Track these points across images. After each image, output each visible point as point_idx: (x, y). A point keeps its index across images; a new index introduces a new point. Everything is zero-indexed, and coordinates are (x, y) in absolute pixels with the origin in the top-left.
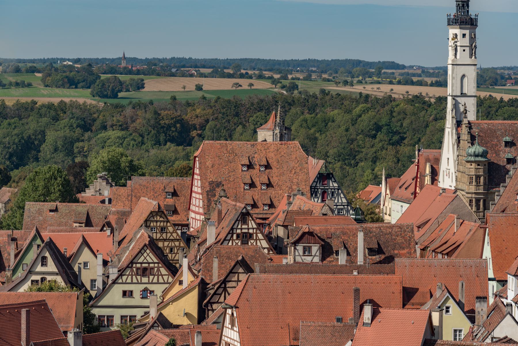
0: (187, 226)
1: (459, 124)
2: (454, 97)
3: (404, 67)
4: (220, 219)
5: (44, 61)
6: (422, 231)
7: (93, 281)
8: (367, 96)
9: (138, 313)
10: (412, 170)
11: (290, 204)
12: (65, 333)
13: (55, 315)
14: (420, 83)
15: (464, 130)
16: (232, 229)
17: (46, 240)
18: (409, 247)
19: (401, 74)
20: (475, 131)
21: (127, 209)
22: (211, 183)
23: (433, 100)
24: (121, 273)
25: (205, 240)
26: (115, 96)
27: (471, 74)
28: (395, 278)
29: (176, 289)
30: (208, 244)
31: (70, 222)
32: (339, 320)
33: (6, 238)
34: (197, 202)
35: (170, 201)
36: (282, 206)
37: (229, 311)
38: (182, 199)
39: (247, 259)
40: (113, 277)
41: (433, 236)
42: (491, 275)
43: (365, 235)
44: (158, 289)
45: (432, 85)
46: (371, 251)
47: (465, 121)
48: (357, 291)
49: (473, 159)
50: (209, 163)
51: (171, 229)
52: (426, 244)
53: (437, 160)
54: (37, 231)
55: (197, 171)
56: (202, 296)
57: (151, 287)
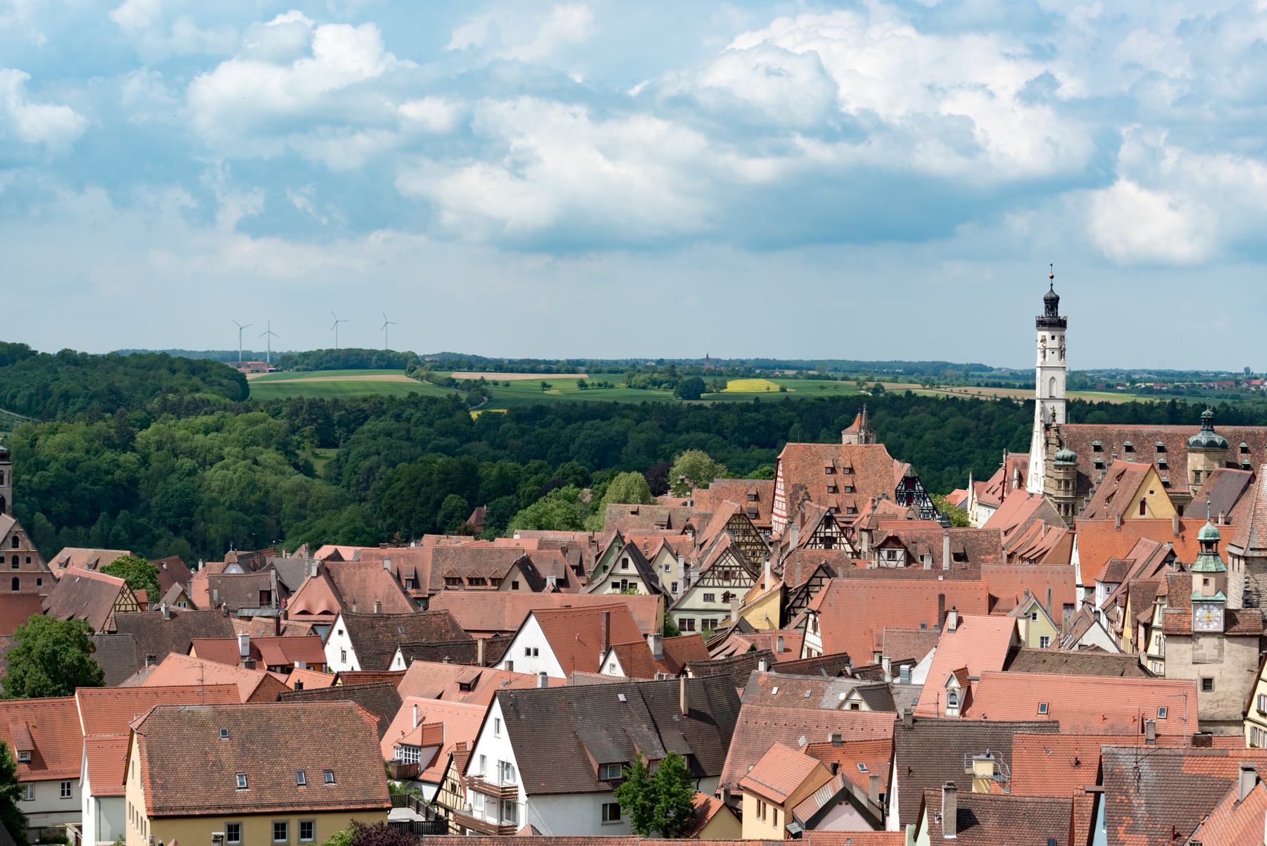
0: (770, 529)
1: (1047, 427)
2: (1042, 401)
3: (991, 369)
4: (803, 524)
5: (627, 362)
7: (675, 585)
8: (954, 398)
9: (720, 617)
10: (999, 476)
11: (874, 508)
12: (646, 636)
13: (637, 617)
14: (1008, 386)
15: (1053, 433)
16: (815, 533)
17: (627, 541)
18: (995, 552)
19: (989, 377)
20: (1064, 434)
21: (709, 511)
22: (794, 486)
23: (1021, 403)
24: (703, 576)
25: (788, 544)
26: (698, 398)
27: (1061, 377)
28: (981, 584)
29: (759, 594)
30: (791, 548)
31: (652, 524)
32: (923, 626)
33: (587, 540)
34: (781, 506)
35: (753, 504)
36: (866, 510)
37: (812, 616)
38: (765, 501)
39: (830, 563)
40: (693, 580)
41: (1020, 542)
42: (1079, 581)
43: (951, 540)
44: (740, 593)
45: (1020, 387)
46: (958, 557)
47: (1054, 425)
48: (942, 597)
49: (1061, 463)
50: (792, 466)
51: (753, 532)
52: (1013, 549)
53: (1025, 465)
54: (619, 533)
55: (780, 473)
56: (784, 601)
57: (732, 591)
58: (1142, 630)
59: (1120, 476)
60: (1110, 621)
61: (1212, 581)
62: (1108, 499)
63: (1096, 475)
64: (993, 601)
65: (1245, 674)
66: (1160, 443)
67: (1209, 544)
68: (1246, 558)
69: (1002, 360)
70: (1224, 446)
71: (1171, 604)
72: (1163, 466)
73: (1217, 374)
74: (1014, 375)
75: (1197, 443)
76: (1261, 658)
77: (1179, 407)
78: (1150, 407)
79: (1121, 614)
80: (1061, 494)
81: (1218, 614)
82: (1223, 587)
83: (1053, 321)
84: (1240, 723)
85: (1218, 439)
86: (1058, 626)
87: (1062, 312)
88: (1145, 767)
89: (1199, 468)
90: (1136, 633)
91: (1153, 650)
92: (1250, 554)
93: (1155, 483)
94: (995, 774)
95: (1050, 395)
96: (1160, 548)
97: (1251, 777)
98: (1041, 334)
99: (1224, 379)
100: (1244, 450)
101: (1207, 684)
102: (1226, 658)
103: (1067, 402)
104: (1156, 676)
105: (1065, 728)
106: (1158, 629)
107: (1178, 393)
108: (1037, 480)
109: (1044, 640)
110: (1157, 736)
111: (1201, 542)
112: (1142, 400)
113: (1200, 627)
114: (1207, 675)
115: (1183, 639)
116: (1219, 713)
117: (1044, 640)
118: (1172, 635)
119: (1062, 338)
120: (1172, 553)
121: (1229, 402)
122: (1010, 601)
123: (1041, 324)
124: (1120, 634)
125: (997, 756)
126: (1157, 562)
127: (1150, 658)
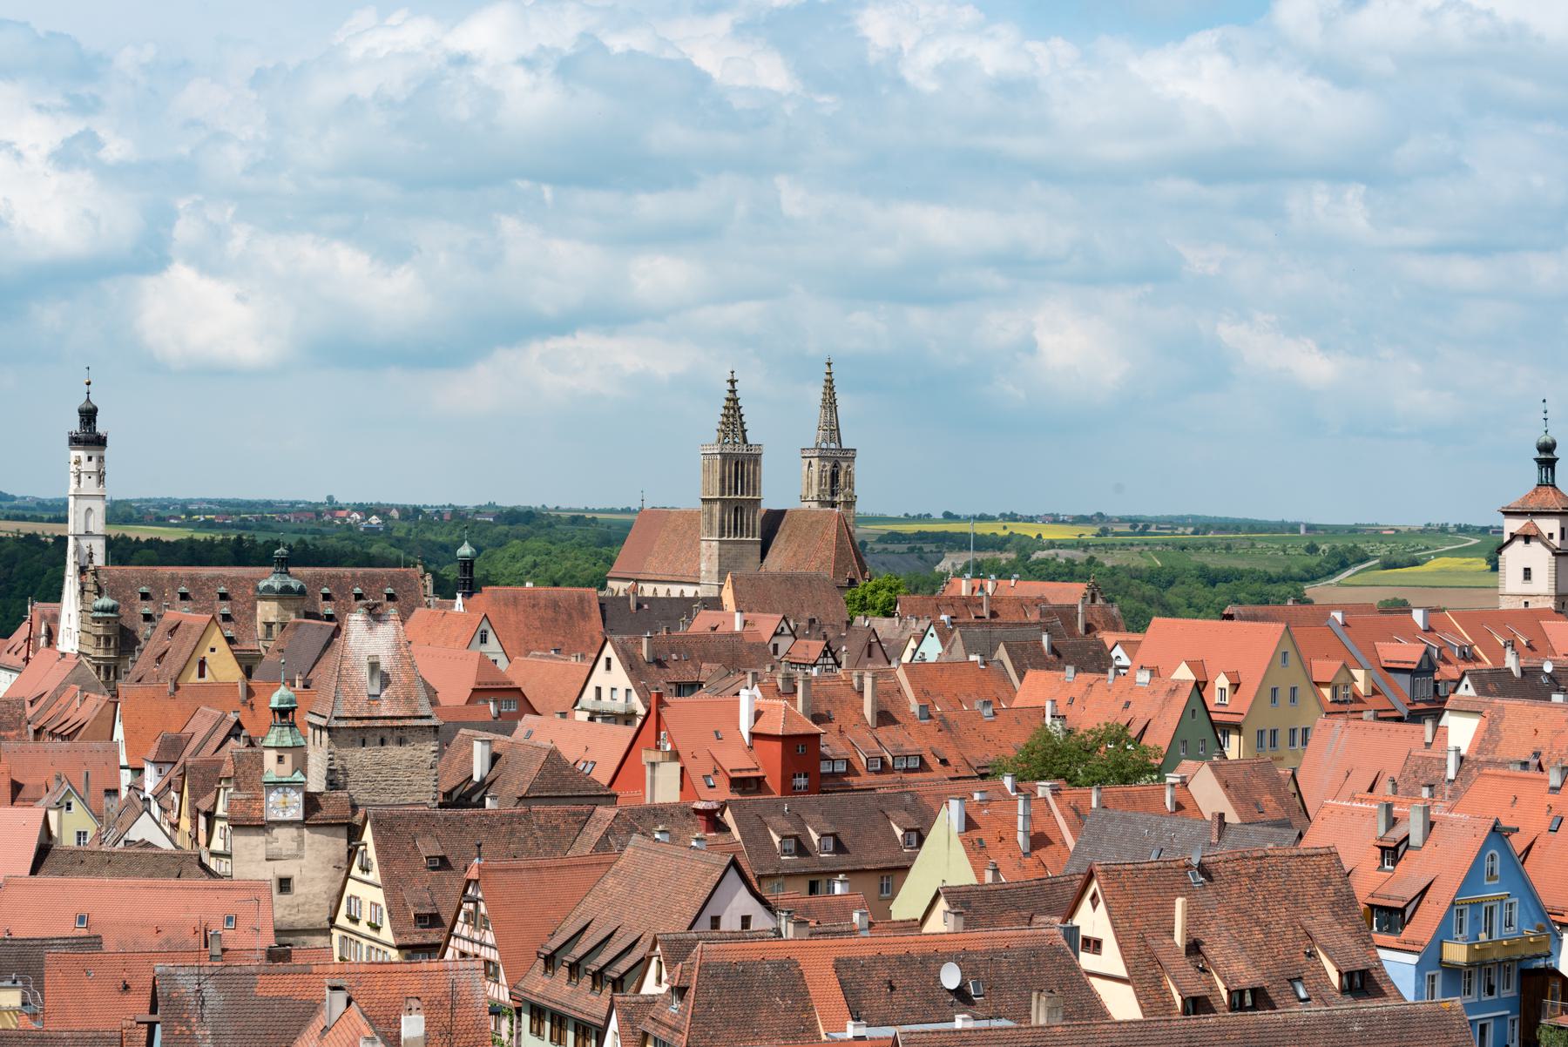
1: (82, 571)
2: (77, 537)
3: (13, 498)
6: (37, 707)
10: (23, 631)
15: (90, 578)
19: (11, 508)
20: (103, 579)
23: (50, 540)
27: (99, 508)
41: (51, 713)
42: (123, 761)
45: (50, 521)
47: (91, 567)
49: (100, 614)
52: (41, 723)
53: (55, 618)
58: (202, 820)
59: (172, 632)
60: (163, 810)
61: (288, 757)
62: (159, 659)
63: (143, 629)
64: (16, 788)
65: (331, 871)
66: (222, 589)
67: (283, 713)
68: (329, 729)
69: (27, 487)
70: (302, 592)
71: (238, 788)
72: (227, 618)
73: (293, 504)
74: (42, 505)
75: (269, 588)
76: (350, 851)
77: (246, 545)
78: (210, 544)
79: (177, 801)
80: (100, 654)
81: (299, 797)
82: (301, 765)
83: (89, 438)
84: (326, 932)
85: (294, 584)
86: (98, 817)
87: (101, 427)
88: (209, 990)
89: (272, 619)
90: (195, 824)
91: (217, 845)
92: (334, 724)
93: (217, 639)
94: (24, 1004)
95: (86, 530)
96: (224, 718)
97: (340, 998)
98: (74, 454)
99: (302, 510)
100: (327, 597)
101: (285, 884)
102: (307, 853)
103: (108, 538)
104: (221, 877)
105: (109, 944)
106: (222, 818)
107: (245, 527)
108: (70, 636)
109: (81, 835)
110: (224, 950)
111: (274, 710)
112: (200, 536)
113: (274, 815)
114: (285, 873)
115: (253, 831)
116: (300, 919)
117: (81, 835)
118: (241, 826)
119: (101, 459)
120: (238, 725)
121: (308, 538)
122: (38, 787)
123: (75, 441)
124: (175, 826)
125: (26, 982)
126: (220, 735)
127: (213, 854)
